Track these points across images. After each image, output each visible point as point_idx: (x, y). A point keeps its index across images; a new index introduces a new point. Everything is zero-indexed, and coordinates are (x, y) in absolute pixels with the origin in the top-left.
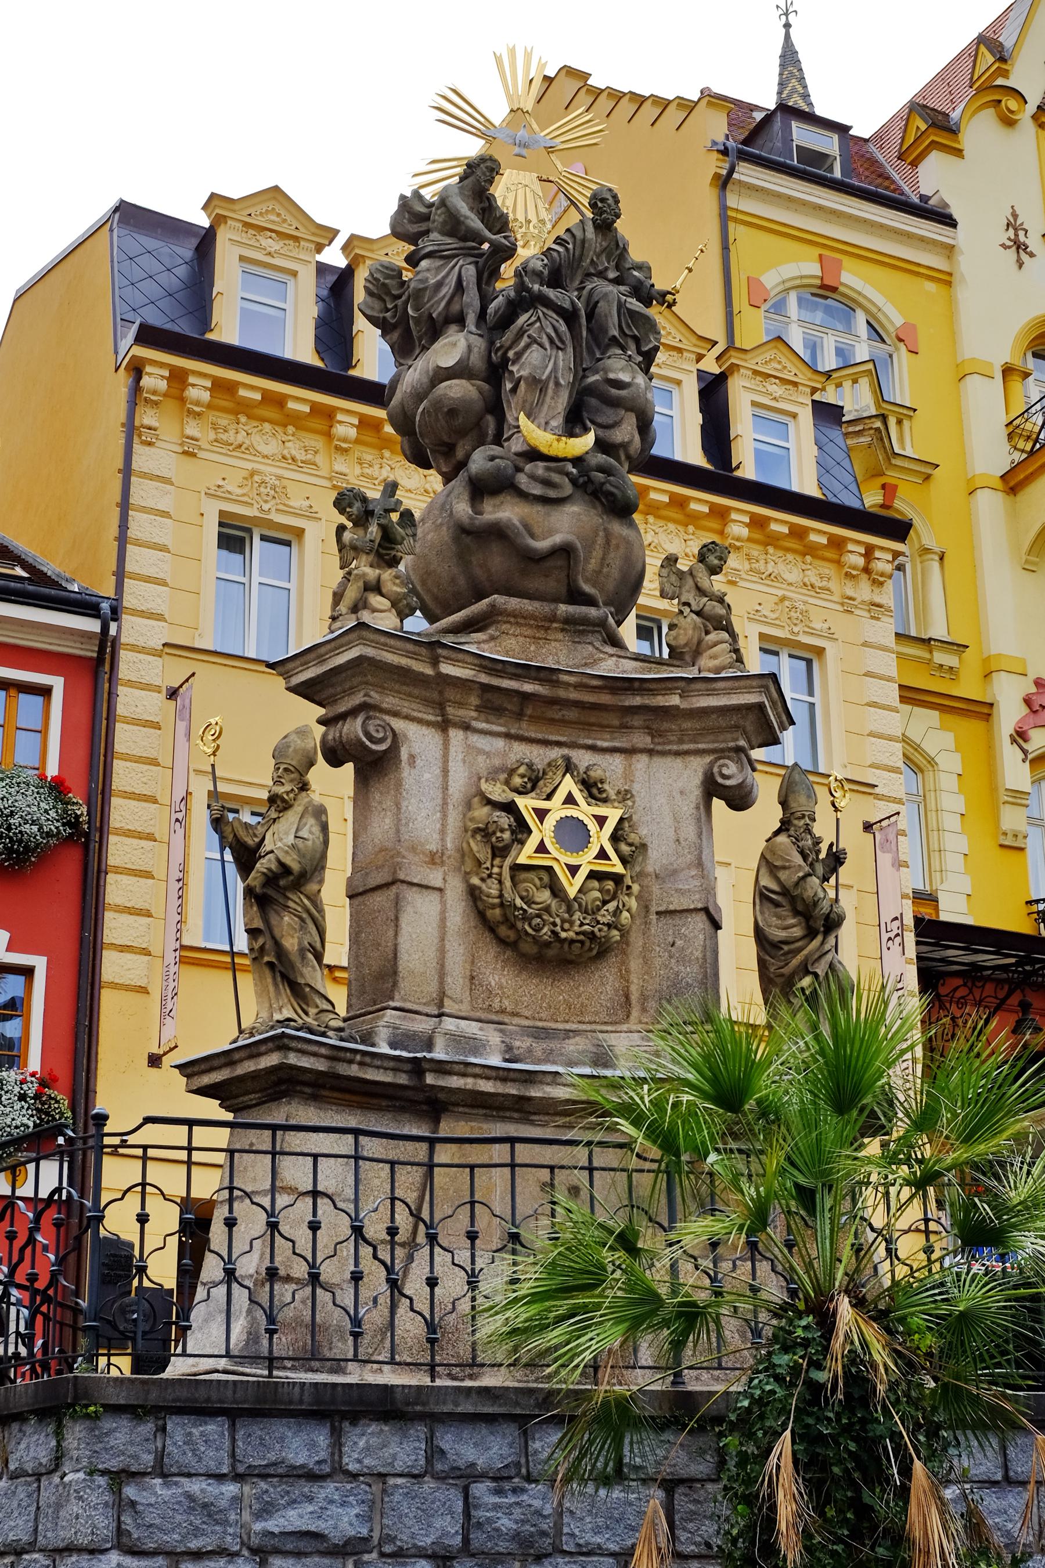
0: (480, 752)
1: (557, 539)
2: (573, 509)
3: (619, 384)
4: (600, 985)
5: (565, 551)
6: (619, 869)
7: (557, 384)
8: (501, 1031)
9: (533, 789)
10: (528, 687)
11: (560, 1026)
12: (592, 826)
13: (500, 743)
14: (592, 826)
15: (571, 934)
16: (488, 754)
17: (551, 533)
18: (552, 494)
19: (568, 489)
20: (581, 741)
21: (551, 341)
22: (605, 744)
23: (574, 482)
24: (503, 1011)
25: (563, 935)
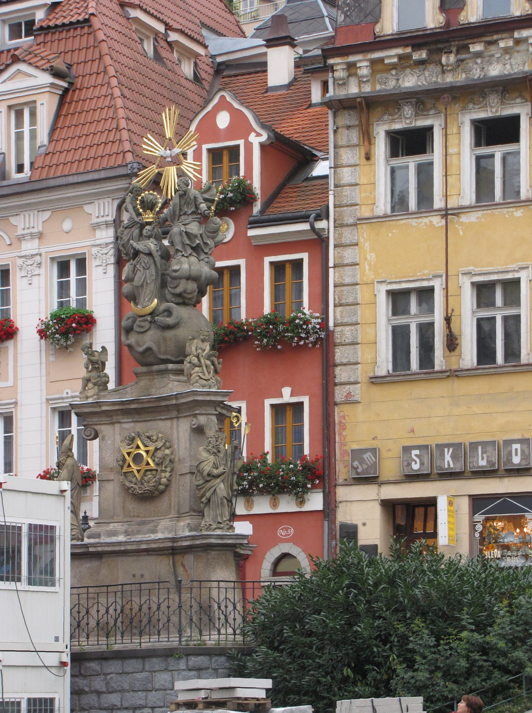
0: (126, 429)
1: (145, 347)
2: (150, 333)
3: (176, 271)
4: (163, 503)
5: (149, 349)
6: (155, 468)
7: (147, 283)
8: (129, 525)
9: (132, 443)
10: (133, 406)
11: (147, 519)
12: (144, 454)
13: (132, 425)
14: (144, 454)
15: (142, 492)
16: (128, 429)
17: (144, 344)
18: (142, 330)
19: (147, 325)
20: (156, 418)
21: (144, 267)
22: (163, 418)
23: (151, 322)
24: (134, 516)
25: (140, 492)
